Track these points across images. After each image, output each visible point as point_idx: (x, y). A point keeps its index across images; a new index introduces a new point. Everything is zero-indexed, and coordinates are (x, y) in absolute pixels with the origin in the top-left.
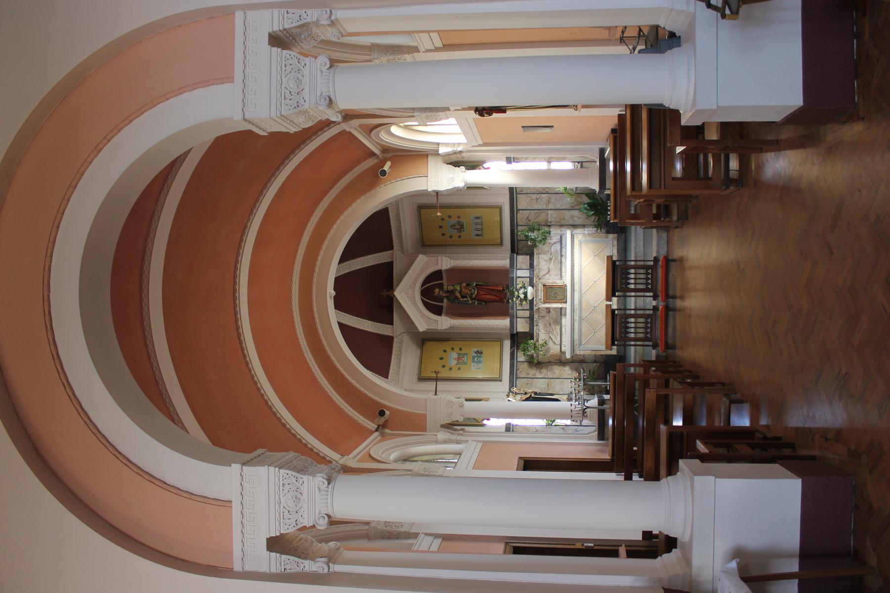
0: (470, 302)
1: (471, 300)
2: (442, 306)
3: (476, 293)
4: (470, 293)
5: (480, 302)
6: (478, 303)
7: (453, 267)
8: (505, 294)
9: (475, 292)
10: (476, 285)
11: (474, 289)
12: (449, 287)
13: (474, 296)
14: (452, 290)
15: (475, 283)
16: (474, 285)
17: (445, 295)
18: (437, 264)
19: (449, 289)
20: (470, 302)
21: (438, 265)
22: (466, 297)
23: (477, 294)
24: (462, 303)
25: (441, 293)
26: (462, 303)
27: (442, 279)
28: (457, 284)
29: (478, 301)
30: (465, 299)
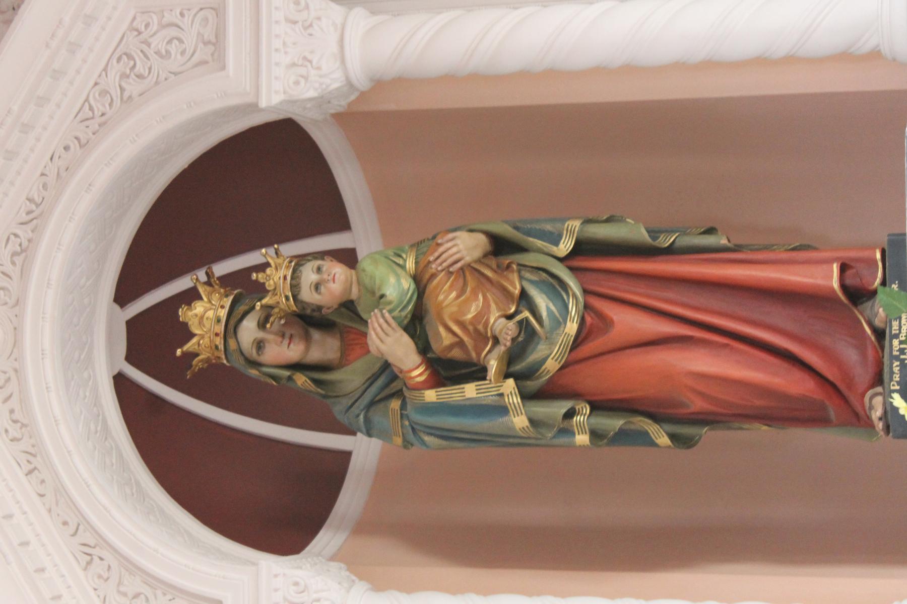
0: (520, 421)
1: (527, 397)
2: (346, 456)
3: (572, 327)
4: (507, 330)
5: (614, 423)
6: (595, 435)
7: (380, 85)
8: (880, 334)
9: (559, 323)
10: (583, 248)
11: (555, 287)
12: (309, 275)
13: (551, 366)
14: (348, 306)
15: (576, 224)
16: (565, 247)
17: (293, 352)
18: (217, 43)
19: (308, 295)
20: (520, 421)
21: (223, 68)
22: (478, 373)
23: (579, 340)
24: (446, 435)
25: (249, 330)
26: (446, 435)
27: (342, 223)
28: (412, 246)
29: (597, 407)
30: (470, 390)
